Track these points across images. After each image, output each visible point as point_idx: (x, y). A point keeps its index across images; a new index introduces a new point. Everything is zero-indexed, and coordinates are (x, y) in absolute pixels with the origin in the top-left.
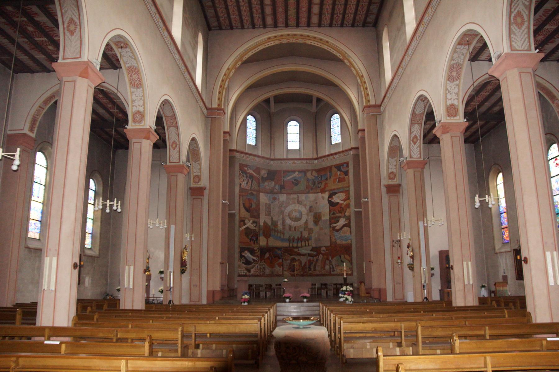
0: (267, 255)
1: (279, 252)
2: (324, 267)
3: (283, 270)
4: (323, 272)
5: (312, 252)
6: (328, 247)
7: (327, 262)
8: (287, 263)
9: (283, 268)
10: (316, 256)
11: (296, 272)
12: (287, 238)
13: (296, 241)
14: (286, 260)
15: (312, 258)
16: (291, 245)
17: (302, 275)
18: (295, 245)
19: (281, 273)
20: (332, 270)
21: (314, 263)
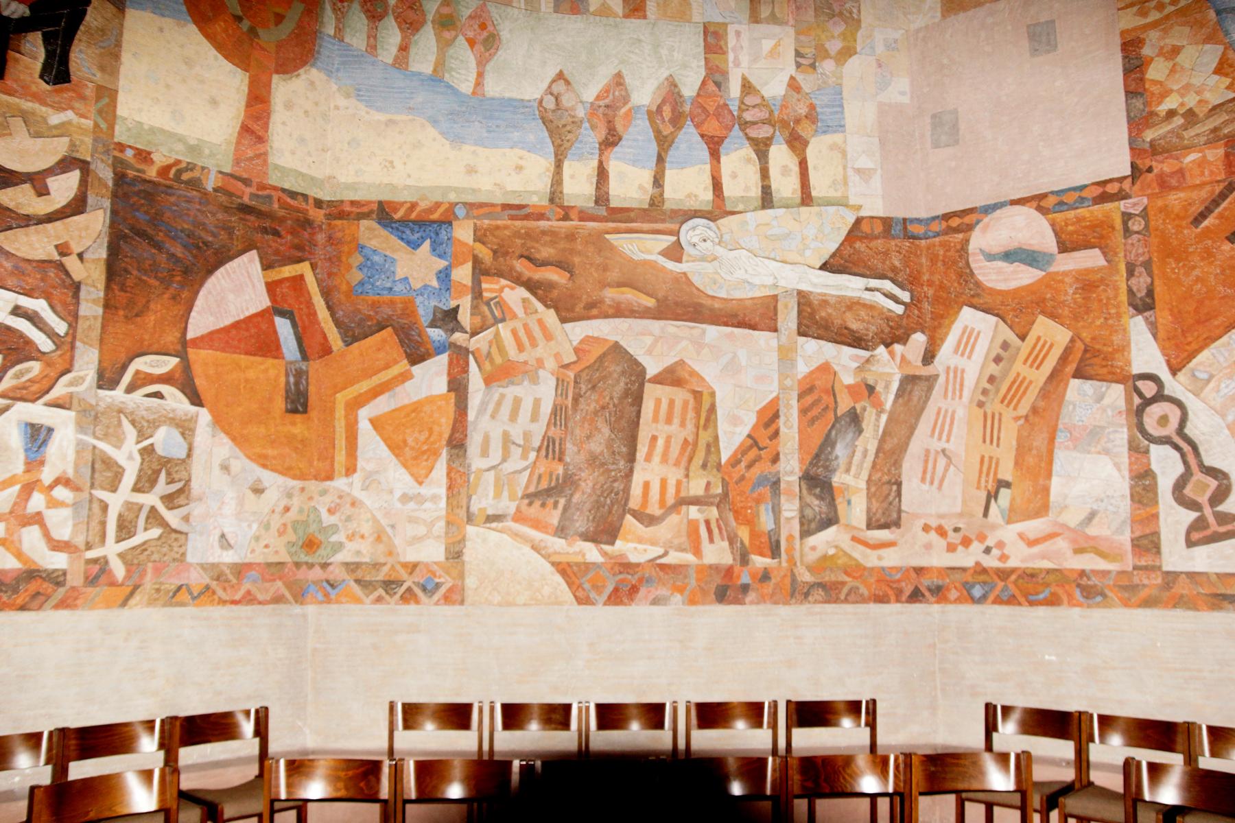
0: (236, 290)
1: (414, 268)
2: (1037, 465)
3: (460, 514)
4: (1014, 544)
5: (851, 286)
6: (1105, 192)
7: (1093, 404)
8: (512, 418)
9: (458, 485)
10: (894, 334)
11: (635, 546)
12: (533, 91)
13: (638, 136)
14: (500, 374)
15: (845, 359)
16: (578, 185)
17: (727, 589)
18: (630, 182)
19: (433, 552)
20: (1174, 520)
21: (874, 424)
